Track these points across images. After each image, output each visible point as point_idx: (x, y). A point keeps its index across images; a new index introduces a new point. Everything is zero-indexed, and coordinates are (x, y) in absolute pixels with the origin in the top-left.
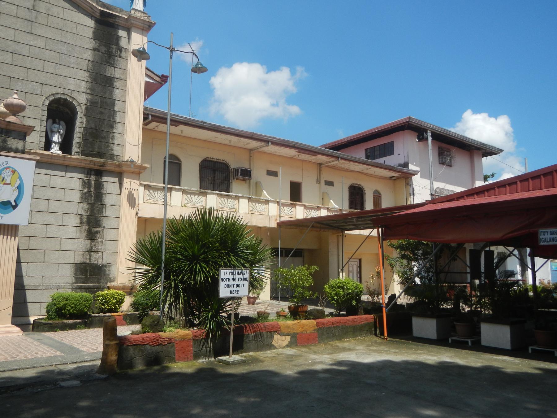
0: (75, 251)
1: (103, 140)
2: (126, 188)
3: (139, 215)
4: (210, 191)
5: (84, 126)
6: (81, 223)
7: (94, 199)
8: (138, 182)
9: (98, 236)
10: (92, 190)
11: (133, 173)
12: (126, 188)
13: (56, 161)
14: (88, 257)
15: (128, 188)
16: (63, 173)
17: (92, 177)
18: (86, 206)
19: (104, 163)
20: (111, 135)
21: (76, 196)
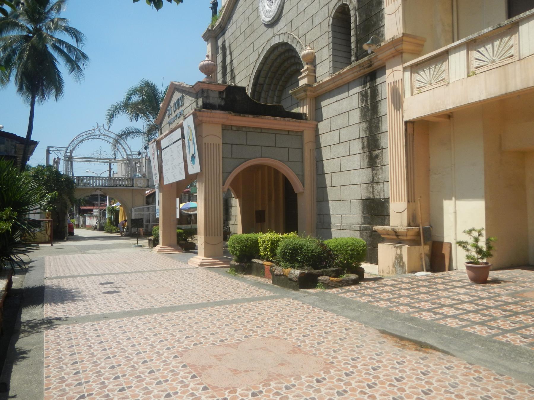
0: (361, 184)
1: (374, 30)
2: (388, 84)
3: (406, 119)
4: (522, 15)
5: (358, 23)
6: (363, 148)
7: (371, 113)
8: (400, 67)
9: (378, 161)
10: (369, 101)
11: (394, 57)
12: (388, 84)
13: (338, 83)
14: (371, 190)
15: (391, 83)
16: (345, 94)
17: (368, 84)
18: (364, 125)
19: (370, 60)
20: (381, 14)
21: (356, 116)
